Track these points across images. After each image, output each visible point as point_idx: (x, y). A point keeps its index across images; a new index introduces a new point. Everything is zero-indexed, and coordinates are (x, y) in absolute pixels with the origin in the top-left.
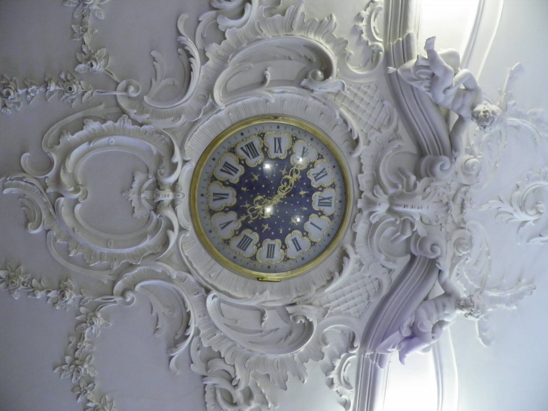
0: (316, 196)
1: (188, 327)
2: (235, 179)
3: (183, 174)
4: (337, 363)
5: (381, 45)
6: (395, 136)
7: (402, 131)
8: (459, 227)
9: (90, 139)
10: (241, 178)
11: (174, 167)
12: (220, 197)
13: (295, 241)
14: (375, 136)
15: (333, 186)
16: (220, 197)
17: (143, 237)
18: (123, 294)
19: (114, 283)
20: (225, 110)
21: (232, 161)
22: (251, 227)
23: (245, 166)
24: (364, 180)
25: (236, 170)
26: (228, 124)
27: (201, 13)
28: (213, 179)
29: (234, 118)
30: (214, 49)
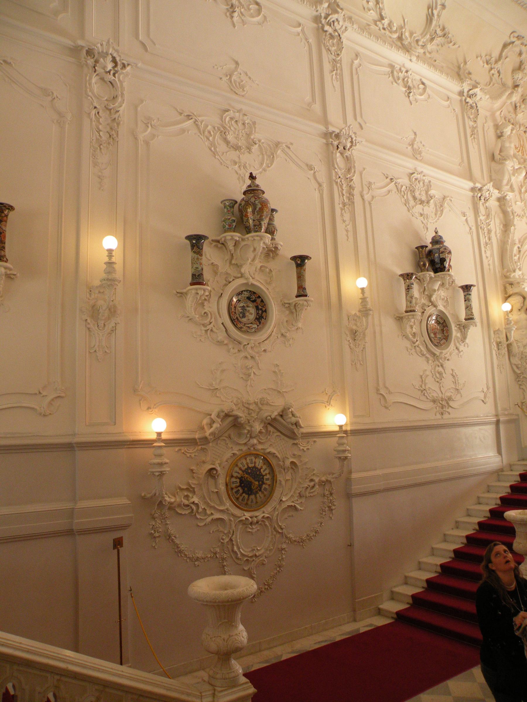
0: (250, 465)
1: (292, 506)
2: (246, 496)
3: (247, 515)
4: (302, 448)
5: (200, 447)
6: (229, 437)
7: (226, 435)
8: (256, 403)
9: (239, 548)
10: (246, 494)
11: (246, 519)
12: (252, 502)
13: (264, 471)
14: (230, 445)
15: (246, 459)
16: (252, 502)
17: (266, 525)
18: (282, 529)
19: (279, 533)
20: (228, 504)
21: (241, 498)
22: (261, 488)
23: (242, 493)
24: (245, 448)
25: (244, 496)
26: (230, 502)
27: (198, 519)
28: (247, 504)
29: (228, 500)
30: (208, 512)
